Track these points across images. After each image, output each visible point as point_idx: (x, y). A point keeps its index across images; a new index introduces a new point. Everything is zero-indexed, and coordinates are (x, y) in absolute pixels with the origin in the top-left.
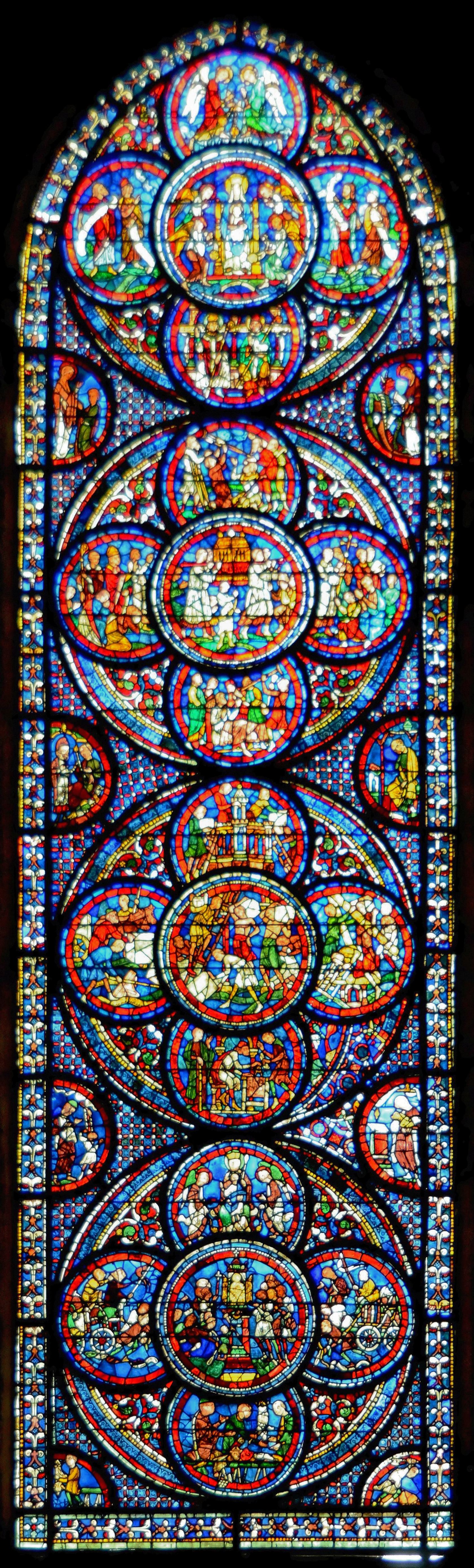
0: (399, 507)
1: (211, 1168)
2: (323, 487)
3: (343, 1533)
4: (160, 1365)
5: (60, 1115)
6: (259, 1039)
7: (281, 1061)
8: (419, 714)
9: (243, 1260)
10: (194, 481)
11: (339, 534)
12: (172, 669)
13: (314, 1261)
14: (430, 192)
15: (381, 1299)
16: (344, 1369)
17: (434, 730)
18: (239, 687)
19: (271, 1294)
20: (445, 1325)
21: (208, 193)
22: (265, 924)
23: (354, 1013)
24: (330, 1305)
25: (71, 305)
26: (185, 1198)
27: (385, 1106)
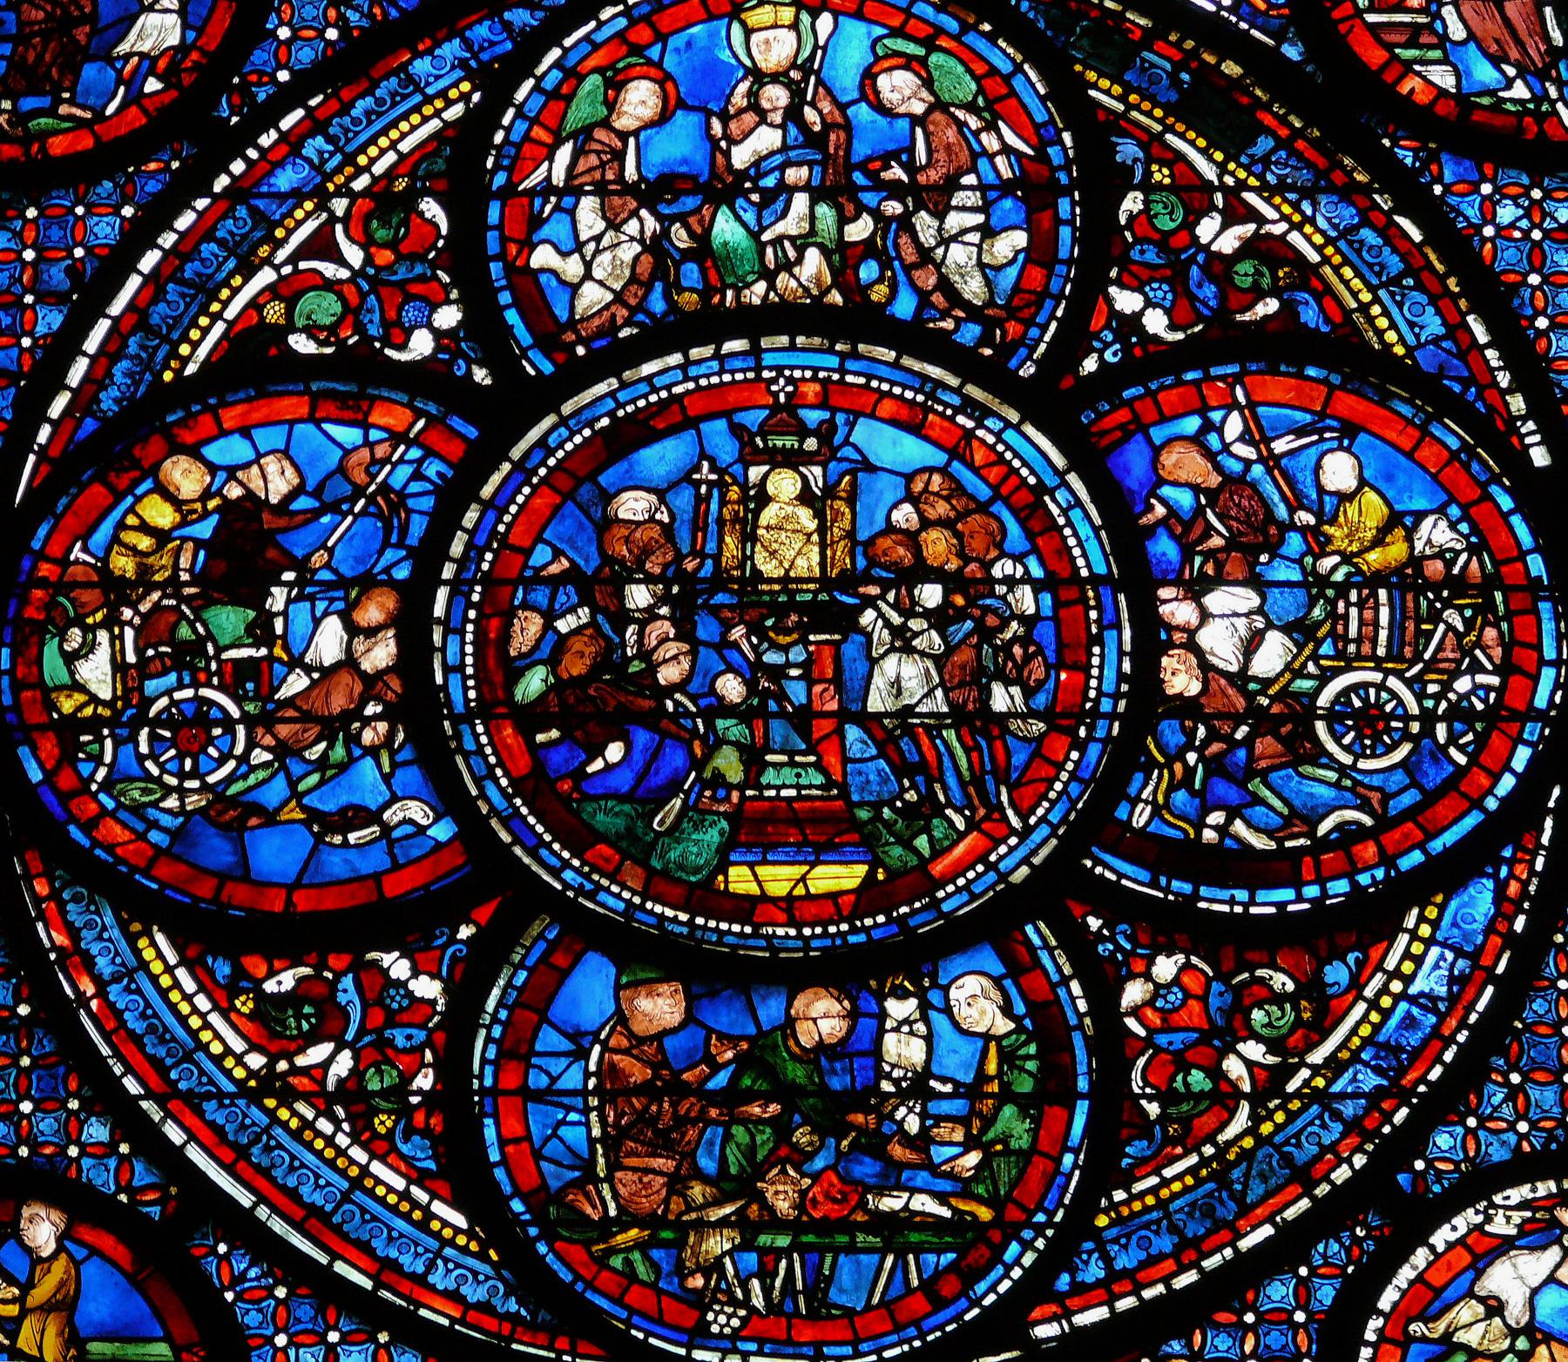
1: (669, 63)
4: (443, 831)
9: (813, 417)
13: (1122, 415)
15: (1416, 561)
16: (1260, 842)
19: (937, 545)
24: (1196, 590)
26: (559, 177)
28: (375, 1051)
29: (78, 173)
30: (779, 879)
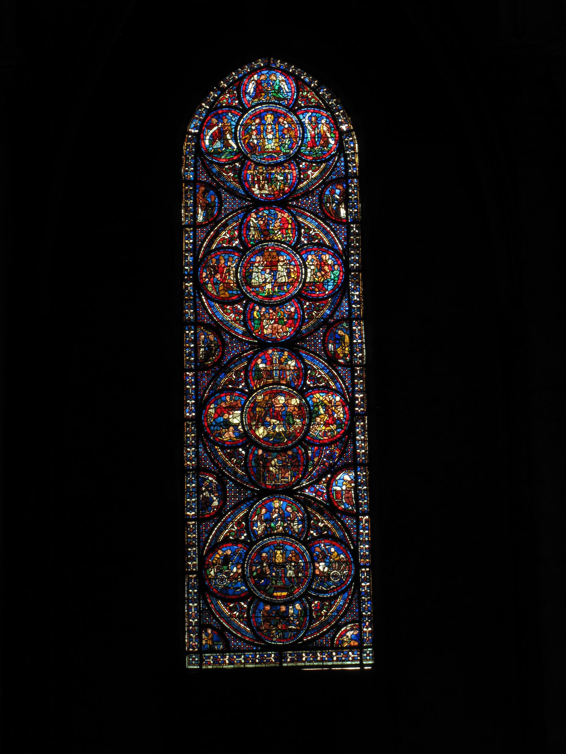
0: (338, 239)
2: (307, 231)
3: (326, 659)
4: (246, 590)
5: (203, 486)
6: (286, 453)
7: (295, 462)
8: (349, 320)
10: (254, 230)
11: (314, 249)
12: (246, 304)
14: (347, 119)
15: (340, 559)
17: (355, 326)
18: (274, 311)
19: (293, 558)
20: (368, 569)
21: (257, 121)
22: (287, 406)
23: (325, 441)
24: (319, 563)
25: (203, 164)
27: (340, 479)
28: (240, 612)
29: (208, 519)
30: (279, 594)
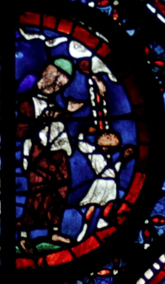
5: (35, 91)
